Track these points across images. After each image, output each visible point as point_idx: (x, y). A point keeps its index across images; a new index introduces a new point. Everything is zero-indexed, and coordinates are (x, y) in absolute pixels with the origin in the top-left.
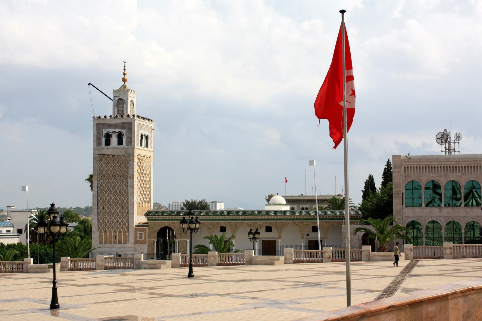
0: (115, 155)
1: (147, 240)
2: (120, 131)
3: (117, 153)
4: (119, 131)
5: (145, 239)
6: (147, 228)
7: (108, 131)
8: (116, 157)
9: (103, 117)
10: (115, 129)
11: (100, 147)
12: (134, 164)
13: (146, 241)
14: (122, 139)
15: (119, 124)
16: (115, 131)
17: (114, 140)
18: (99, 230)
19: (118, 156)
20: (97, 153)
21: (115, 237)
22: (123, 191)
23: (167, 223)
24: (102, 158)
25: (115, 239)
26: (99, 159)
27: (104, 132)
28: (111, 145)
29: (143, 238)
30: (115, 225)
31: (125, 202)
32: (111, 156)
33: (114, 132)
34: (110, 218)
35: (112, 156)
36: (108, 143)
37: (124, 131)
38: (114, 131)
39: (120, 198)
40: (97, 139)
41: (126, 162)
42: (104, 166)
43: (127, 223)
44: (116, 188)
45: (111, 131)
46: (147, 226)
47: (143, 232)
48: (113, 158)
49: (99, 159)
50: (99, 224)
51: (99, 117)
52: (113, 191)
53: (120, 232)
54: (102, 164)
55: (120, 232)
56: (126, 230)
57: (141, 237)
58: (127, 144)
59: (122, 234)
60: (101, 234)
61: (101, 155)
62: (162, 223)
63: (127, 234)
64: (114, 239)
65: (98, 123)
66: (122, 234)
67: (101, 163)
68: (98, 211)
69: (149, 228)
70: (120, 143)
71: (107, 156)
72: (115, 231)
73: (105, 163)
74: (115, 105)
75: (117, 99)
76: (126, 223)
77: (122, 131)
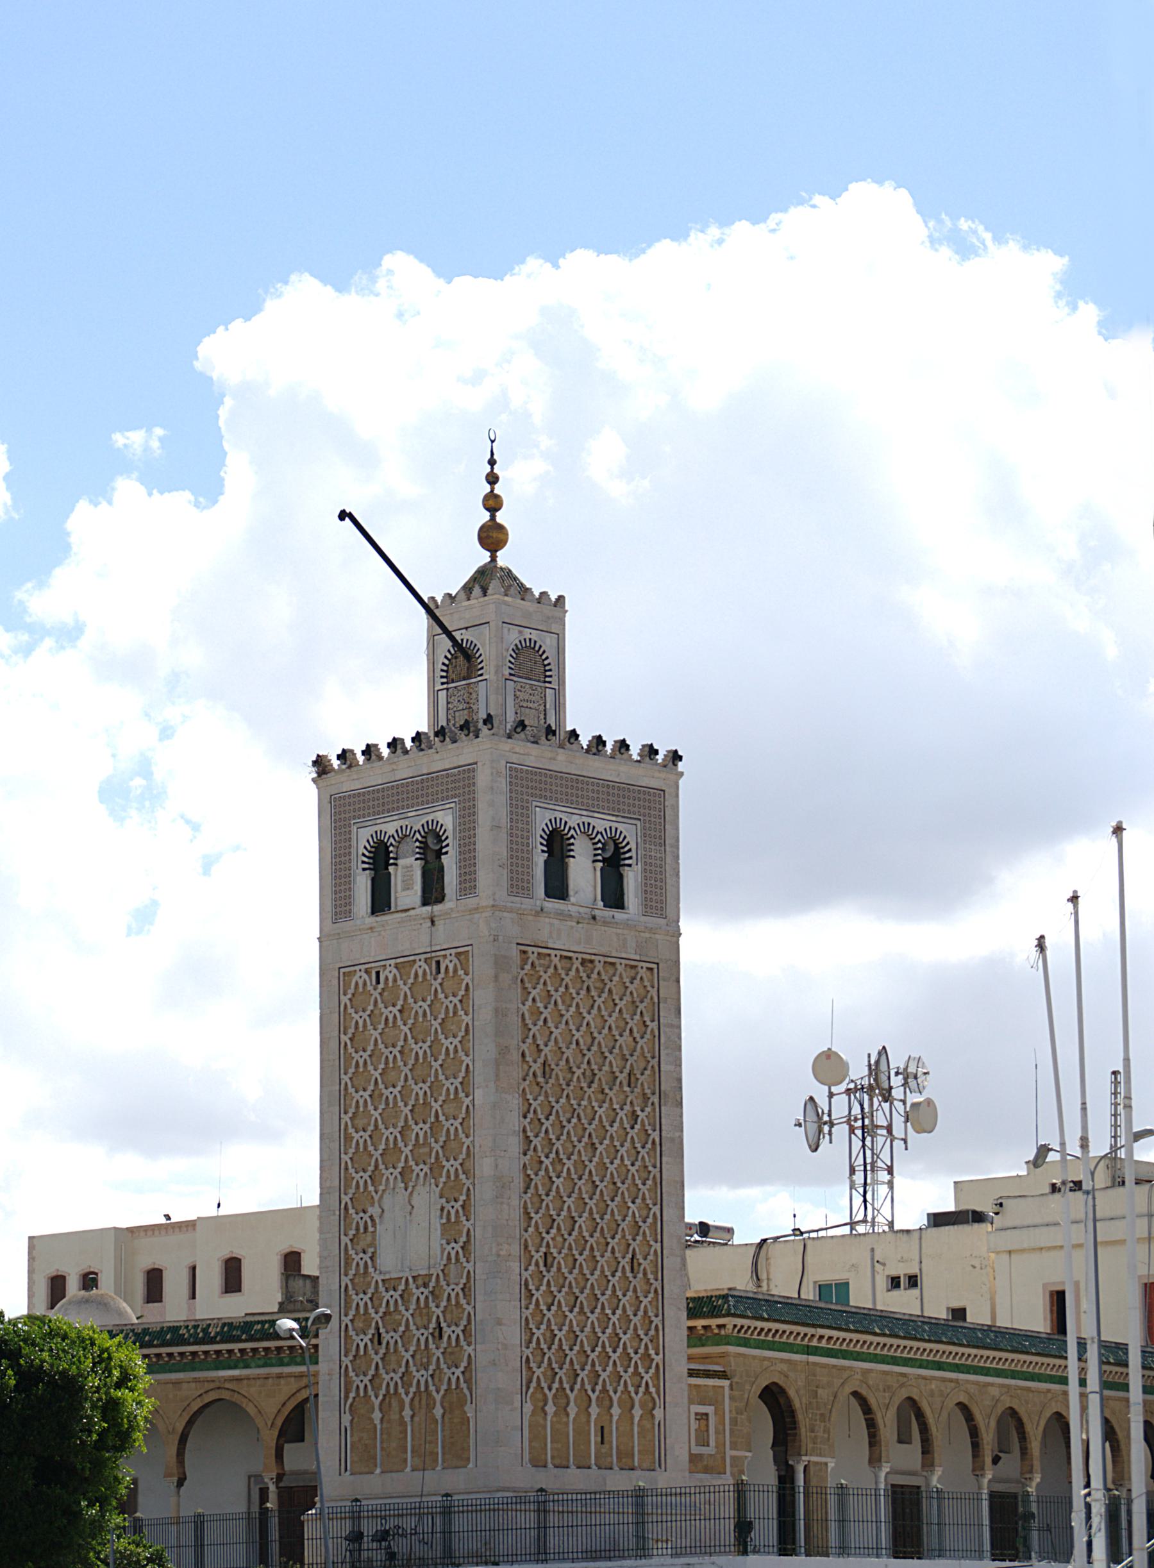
0: (597, 958)
1: (729, 1453)
3: (603, 951)
4: (607, 825)
6: (726, 1383)
7: (559, 815)
8: (599, 973)
11: (527, 904)
14: (621, 877)
15: (608, 785)
16: (593, 822)
17: (583, 873)
18: (531, 1390)
22: (633, 1169)
25: (602, 1443)
26: (523, 969)
27: (542, 819)
28: (572, 899)
29: (712, 1443)
31: (644, 1233)
32: (577, 964)
34: (579, 1318)
35: (583, 962)
37: (629, 832)
38: (586, 820)
42: (546, 1013)
44: (600, 1148)
46: (723, 1375)
47: (709, 1409)
49: (523, 969)
54: (534, 1000)
56: (652, 1390)
63: (658, 1413)
64: (596, 1443)
65: (514, 758)
66: (637, 1412)
67: (534, 993)
71: (556, 960)
72: (605, 1402)
74: (507, 672)
75: (513, 637)
76: (652, 1352)
77: (621, 827)
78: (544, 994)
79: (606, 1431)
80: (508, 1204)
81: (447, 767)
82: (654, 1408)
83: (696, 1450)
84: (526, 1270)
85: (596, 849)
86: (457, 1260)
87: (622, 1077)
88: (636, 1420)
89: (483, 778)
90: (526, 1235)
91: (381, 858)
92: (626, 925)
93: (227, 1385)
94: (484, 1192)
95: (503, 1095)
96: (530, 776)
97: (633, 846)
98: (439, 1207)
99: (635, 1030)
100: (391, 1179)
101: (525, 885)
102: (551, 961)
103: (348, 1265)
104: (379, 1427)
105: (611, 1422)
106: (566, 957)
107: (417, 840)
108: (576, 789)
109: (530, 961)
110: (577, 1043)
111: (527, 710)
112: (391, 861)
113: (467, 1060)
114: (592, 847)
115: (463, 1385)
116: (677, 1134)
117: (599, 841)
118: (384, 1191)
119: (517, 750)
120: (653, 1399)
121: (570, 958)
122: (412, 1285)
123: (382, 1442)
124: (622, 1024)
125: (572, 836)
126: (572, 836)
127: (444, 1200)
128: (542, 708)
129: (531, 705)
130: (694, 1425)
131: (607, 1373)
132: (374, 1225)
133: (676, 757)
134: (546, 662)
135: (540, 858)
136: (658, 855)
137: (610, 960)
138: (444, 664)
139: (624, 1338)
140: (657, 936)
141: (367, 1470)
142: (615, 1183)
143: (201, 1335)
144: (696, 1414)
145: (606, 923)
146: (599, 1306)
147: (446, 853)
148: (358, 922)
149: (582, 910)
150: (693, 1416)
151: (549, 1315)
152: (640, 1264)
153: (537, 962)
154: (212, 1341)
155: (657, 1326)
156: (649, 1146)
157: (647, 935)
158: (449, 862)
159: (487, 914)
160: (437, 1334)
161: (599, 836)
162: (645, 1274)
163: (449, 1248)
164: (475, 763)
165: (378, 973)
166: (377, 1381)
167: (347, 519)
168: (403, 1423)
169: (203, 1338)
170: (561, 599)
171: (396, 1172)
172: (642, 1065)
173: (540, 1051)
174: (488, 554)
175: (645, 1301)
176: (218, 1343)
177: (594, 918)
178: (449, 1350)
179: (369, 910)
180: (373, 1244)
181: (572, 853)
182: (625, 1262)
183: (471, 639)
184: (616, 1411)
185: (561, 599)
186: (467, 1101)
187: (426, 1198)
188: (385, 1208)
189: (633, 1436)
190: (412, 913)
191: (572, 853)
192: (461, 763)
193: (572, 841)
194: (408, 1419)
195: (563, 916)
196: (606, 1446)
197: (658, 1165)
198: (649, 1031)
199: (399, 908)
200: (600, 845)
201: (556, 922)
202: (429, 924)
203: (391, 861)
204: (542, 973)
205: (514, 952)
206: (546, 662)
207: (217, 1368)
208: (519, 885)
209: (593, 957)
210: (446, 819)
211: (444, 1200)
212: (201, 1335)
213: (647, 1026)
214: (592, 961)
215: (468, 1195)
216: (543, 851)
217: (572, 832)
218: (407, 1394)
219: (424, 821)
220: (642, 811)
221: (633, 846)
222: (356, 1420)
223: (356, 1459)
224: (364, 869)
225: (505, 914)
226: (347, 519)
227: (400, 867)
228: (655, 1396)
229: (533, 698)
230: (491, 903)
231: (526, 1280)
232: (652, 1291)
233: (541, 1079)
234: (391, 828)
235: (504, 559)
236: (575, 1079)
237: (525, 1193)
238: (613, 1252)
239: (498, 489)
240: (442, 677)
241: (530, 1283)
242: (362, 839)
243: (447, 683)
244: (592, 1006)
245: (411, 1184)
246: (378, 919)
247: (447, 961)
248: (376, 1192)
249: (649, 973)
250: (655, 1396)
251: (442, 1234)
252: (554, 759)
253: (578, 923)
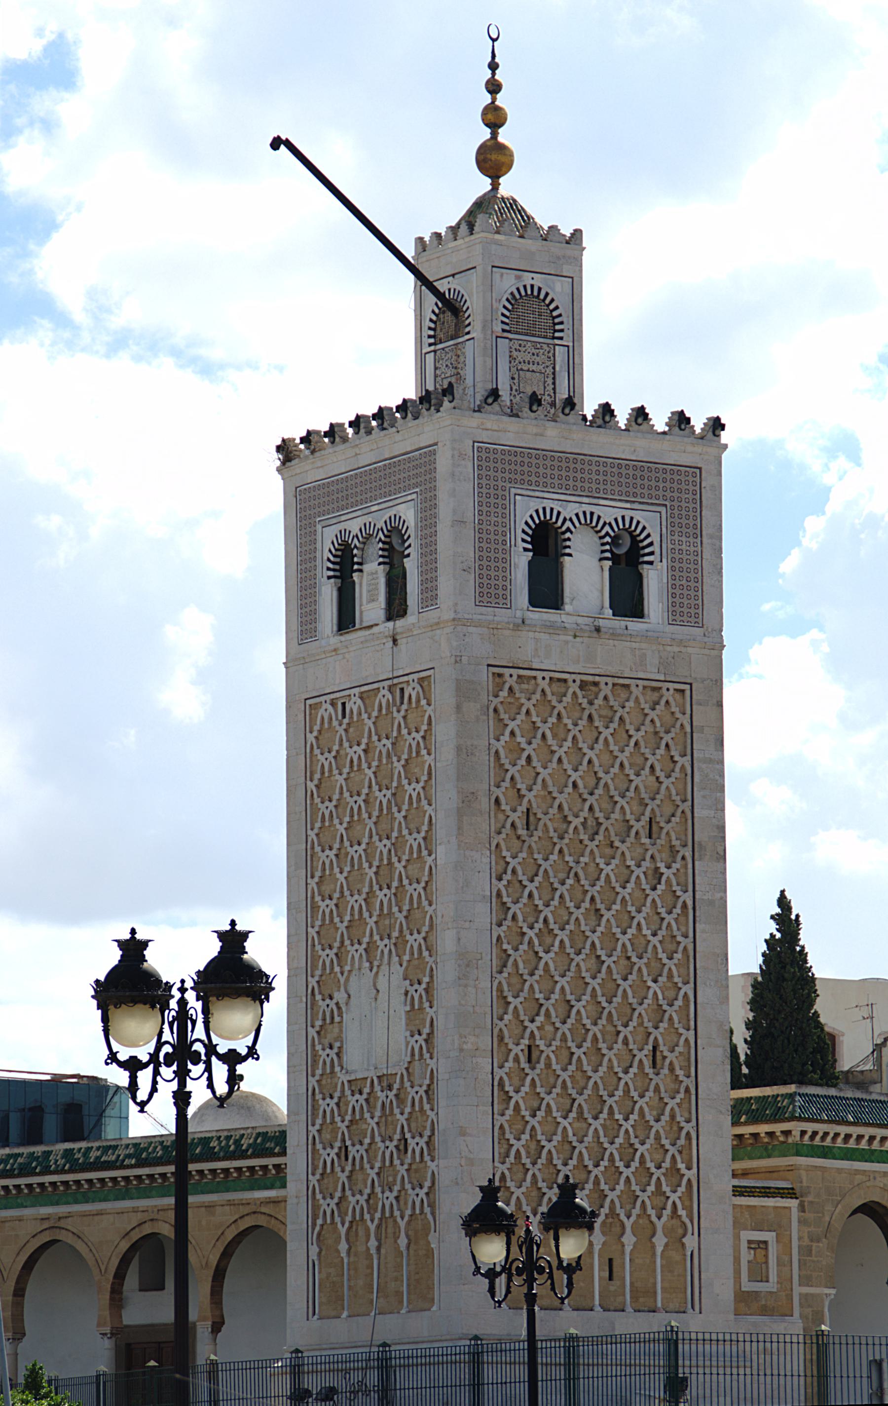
0: (603, 680)
1: (798, 1290)
2: (624, 512)
3: (611, 670)
4: (619, 514)
5: (785, 1282)
6: (793, 1203)
7: (548, 504)
8: (606, 698)
11: (502, 615)
12: (721, 762)
13: (790, 1298)
14: (640, 576)
15: (620, 465)
16: (597, 511)
17: (585, 574)
21: (610, 1261)
22: (655, 941)
24: (511, 689)
25: (611, 1278)
26: (496, 696)
27: (525, 509)
28: (568, 607)
31: (671, 1019)
32: (574, 688)
34: (577, 1125)
35: (583, 685)
36: (547, 591)
37: (650, 522)
38: (588, 509)
40: (481, 549)
41: (667, 738)
42: (529, 750)
43: (689, 1168)
44: (607, 915)
46: (790, 1193)
48: (591, 703)
49: (496, 696)
50: (503, 1168)
52: (595, 937)
54: (512, 733)
56: (682, 1212)
57: (759, 1273)
59: (660, 1241)
61: (507, 672)
62: (859, 1178)
63: (690, 1242)
64: (600, 1278)
66: (660, 1241)
67: (512, 725)
68: (499, 1073)
69: (802, 1208)
70: (627, 599)
71: (544, 684)
73: (536, 729)
74: (498, 328)
75: (507, 284)
76: (681, 1166)
78: (527, 726)
79: (615, 1264)
80: (475, 987)
81: (409, 449)
82: (684, 1235)
83: (747, 1286)
84: (501, 1067)
85: (603, 544)
86: (421, 1055)
87: (640, 826)
88: (659, 1250)
89: (443, 462)
90: (501, 1024)
91: (345, 564)
92: (645, 637)
93: (263, 1209)
94: (446, 972)
95: (468, 853)
96: (507, 458)
97: (655, 538)
98: (403, 991)
99: (658, 768)
100: (357, 956)
101: (501, 592)
102: (537, 685)
103: (315, 1062)
104: (346, 1261)
105: (623, 1253)
106: (559, 680)
107: (380, 540)
108: (573, 472)
109: (507, 686)
110: (575, 785)
111: (529, 374)
112: (356, 567)
113: (429, 810)
114: (599, 542)
115: (427, 1210)
116: (718, 895)
117: (607, 534)
118: (350, 971)
119: (489, 425)
120: (684, 1223)
121: (565, 681)
122: (377, 1088)
123: (349, 1280)
124: (639, 760)
125: (568, 530)
126: (568, 530)
127: (408, 982)
128: (550, 370)
129: (534, 368)
130: (746, 1256)
131: (618, 1192)
132: (340, 1015)
133: (716, 425)
134: (555, 314)
135: (521, 560)
136: (692, 549)
137: (621, 681)
138: (431, 320)
139: (641, 1149)
140: (690, 650)
141: (333, 1313)
142: (629, 958)
143: (232, 1148)
144: (749, 1242)
145: (614, 635)
146: (606, 1111)
147: (408, 555)
148: (323, 642)
149: (580, 620)
150: (744, 1245)
151: (533, 1122)
152: (665, 1058)
153: (516, 687)
154: (243, 1155)
155: (688, 1133)
156: (678, 910)
157: (676, 649)
158: (411, 565)
159: (448, 630)
160: (402, 1147)
161: (607, 528)
162: (672, 1069)
163: (412, 1041)
164: (436, 444)
165: (344, 704)
166: (344, 1204)
167: (282, 147)
168: (369, 1257)
169: (234, 1152)
170: (577, 234)
171: (361, 949)
172: (668, 809)
173: (521, 797)
174: (489, 181)
175: (672, 1103)
176: (250, 1157)
177: (598, 630)
178: (414, 1167)
179: (335, 628)
180: (339, 1038)
181: (567, 551)
182: (643, 1056)
183: (458, 288)
184: (629, 1240)
185: (577, 234)
186: (429, 860)
187: (393, 978)
188: (351, 993)
189: (654, 1271)
190: (375, 630)
191: (567, 551)
192: (422, 445)
193: (568, 535)
194: (373, 1251)
195: (552, 628)
196: (616, 1282)
197: (691, 934)
198: (677, 769)
199: (365, 625)
200: (608, 539)
201: (543, 636)
202: (391, 643)
203: (356, 567)
204: (523, 701)
205: (484, 676)
206: (555, 314)
207: (252, 1189)
208: (491, 591)
209: (597, 679)
210: (408, 514)
211: (408, 982)
212: (232, 1148)
213: (675, 762)
214: (596, 684)
215: (431, 977)
216: (525, 550)
217: (568, 524)
218: (372, 1221)
219: (386, 517)
220: (668, 494)
221: (655, 538)
222: (323, 1253)
223: (324, 1300)
224: (329, 578)
225: (471, 629)
226: (282, 147)
227: (365, 573)
228: (687, 1221)
229: (538, 359)
230: (452, 616)
231: (501, 1079)
232: (682, 1090)
233: (522, 832)
234: (354, 527)
235: (508, 186)
236: (571, 830)
237: (501, 972)
238: (626, 1042)
239: (501, 100)
240: (430, 337)
241: (507, 1083)
242: (327, 540)
243: (435, 344)
244: (597, 739)
245: (376, 963)
246: (342, 638)
247: (410, 688)
248: (342, 974)
249: (678, 696)
250: (687, 1221)
251: (407, 1025)
252: (542, 435)
253: (575, 636)
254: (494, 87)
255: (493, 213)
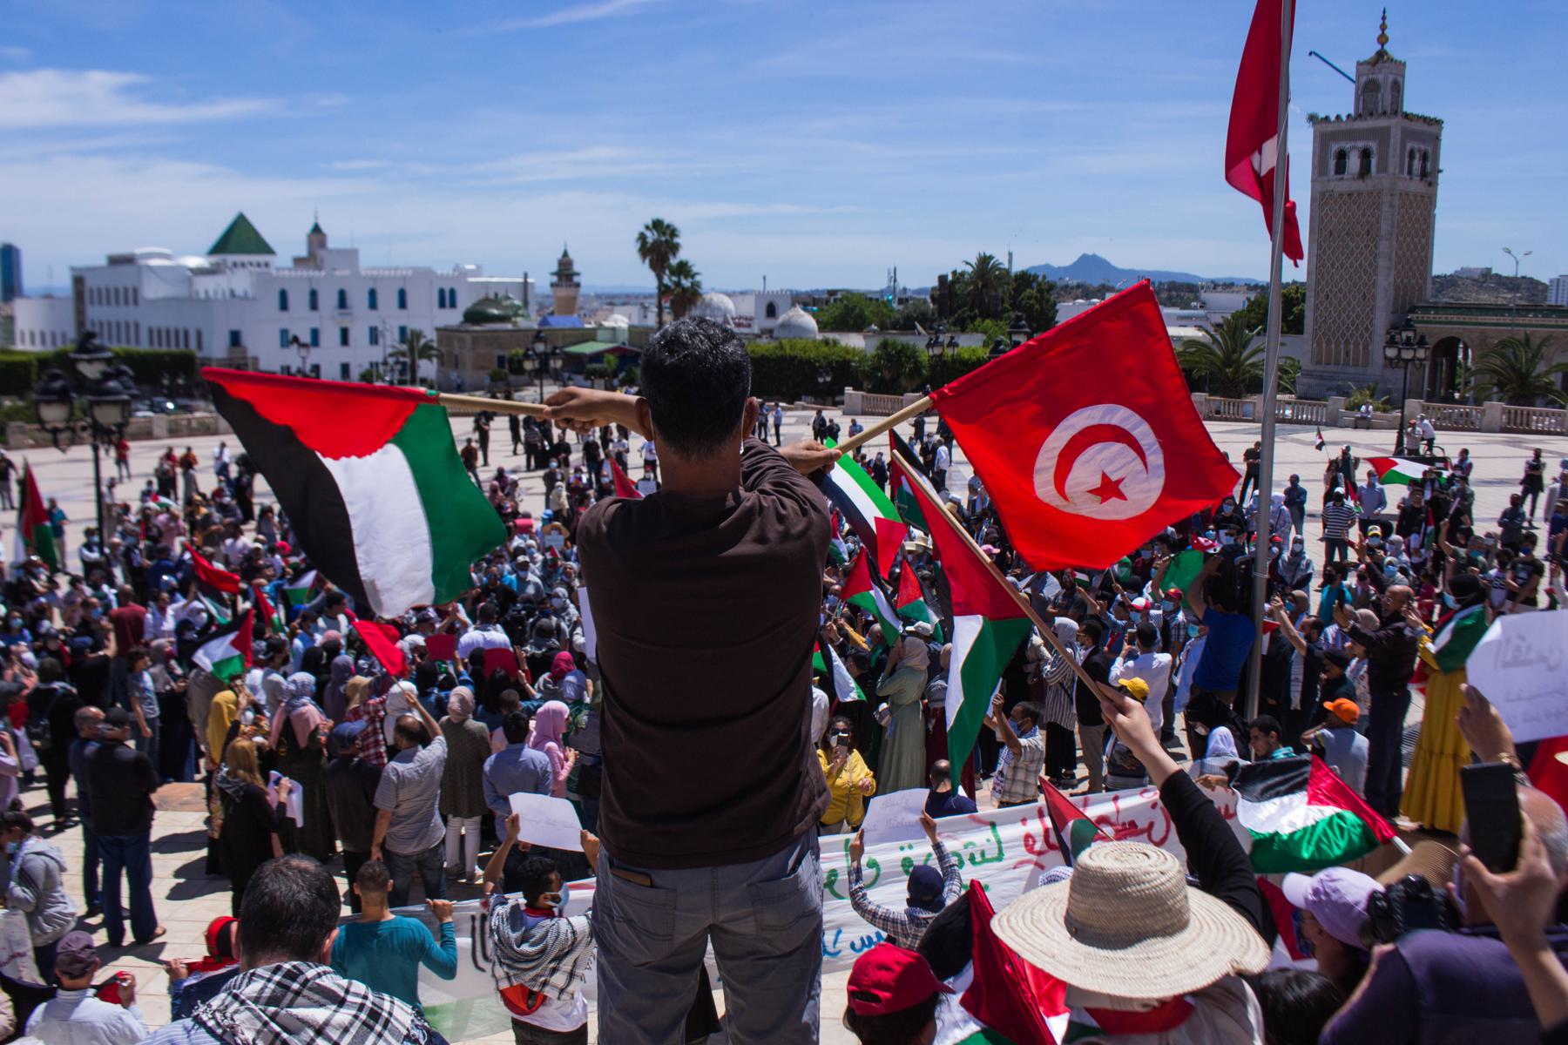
9: (1333, 118)
10: (1355, 140)
17: (1354, 163)
19: (1360, 194)
20: (1319, 188)
23: (1453, 330)
27: (1335, 148)
30: (1348, 329)
33: (1353, 148)
36: (1340, 169)
37: (1373, 145)
39: (1360, 278)
45: (1347, 145)
51: (1327, 118)
53: (1356, 344)
55: (1356, 344)
58: (1378, 171)
60: (1319, 345)
72: (1347, 342)
75: (1363, 80)
254: (1384, 18)
255: (1381, 55)
